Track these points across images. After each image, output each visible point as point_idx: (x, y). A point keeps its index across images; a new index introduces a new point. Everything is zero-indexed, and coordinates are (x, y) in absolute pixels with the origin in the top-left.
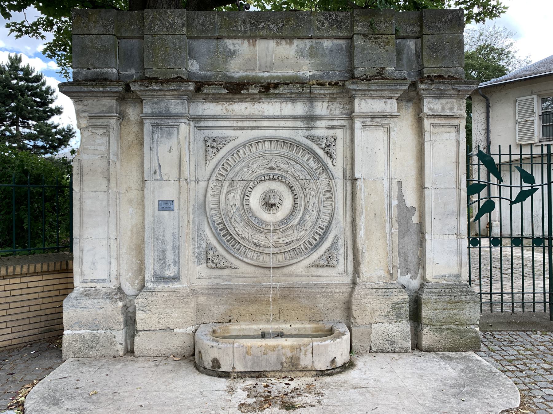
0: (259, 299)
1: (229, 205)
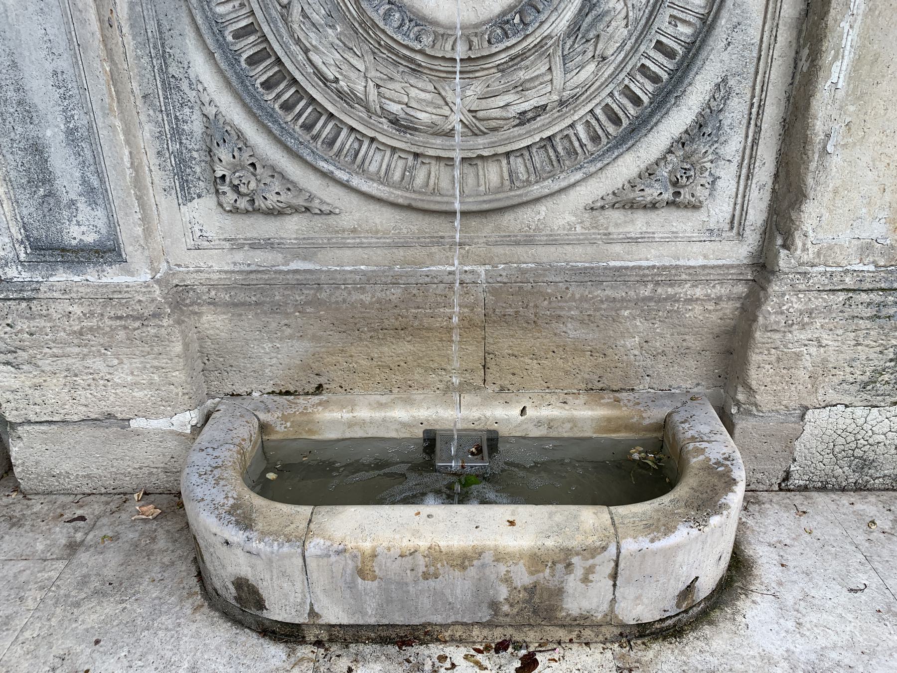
0: (416, 323)
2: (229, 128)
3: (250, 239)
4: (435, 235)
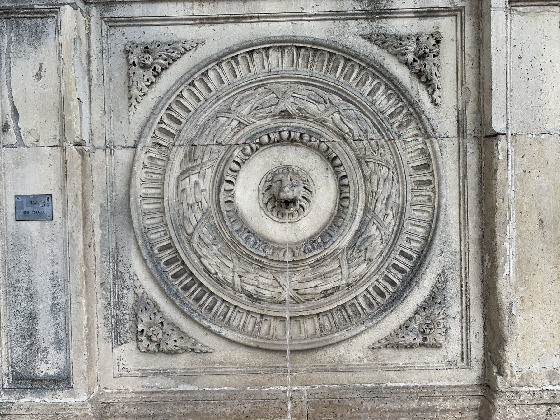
1: (185, 204)
2: (149, 301)
3: (154, 370)
4: (274, 365)
